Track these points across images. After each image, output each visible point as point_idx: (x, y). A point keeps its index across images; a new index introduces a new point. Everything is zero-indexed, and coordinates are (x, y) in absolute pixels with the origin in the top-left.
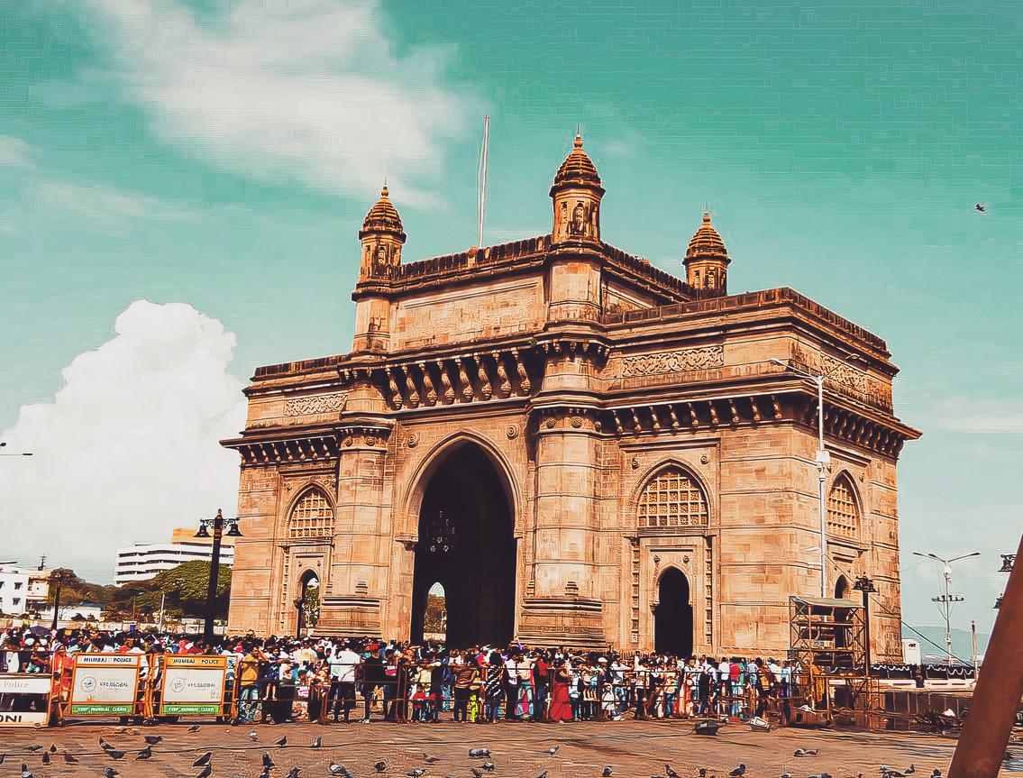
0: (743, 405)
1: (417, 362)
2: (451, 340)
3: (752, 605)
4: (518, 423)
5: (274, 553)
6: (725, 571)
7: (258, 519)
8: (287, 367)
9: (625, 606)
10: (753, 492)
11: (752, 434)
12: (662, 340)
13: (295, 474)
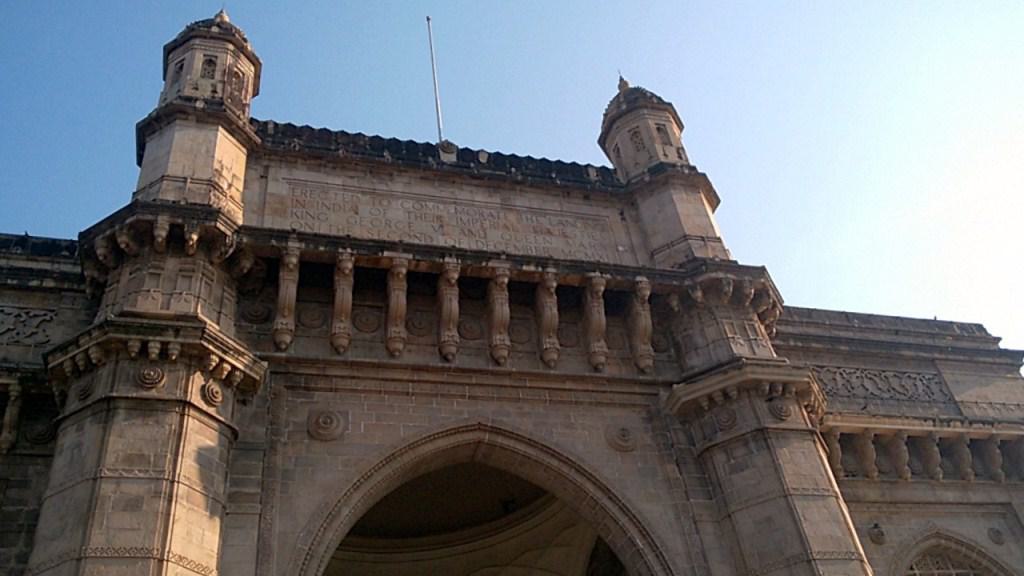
12: (843, 348)
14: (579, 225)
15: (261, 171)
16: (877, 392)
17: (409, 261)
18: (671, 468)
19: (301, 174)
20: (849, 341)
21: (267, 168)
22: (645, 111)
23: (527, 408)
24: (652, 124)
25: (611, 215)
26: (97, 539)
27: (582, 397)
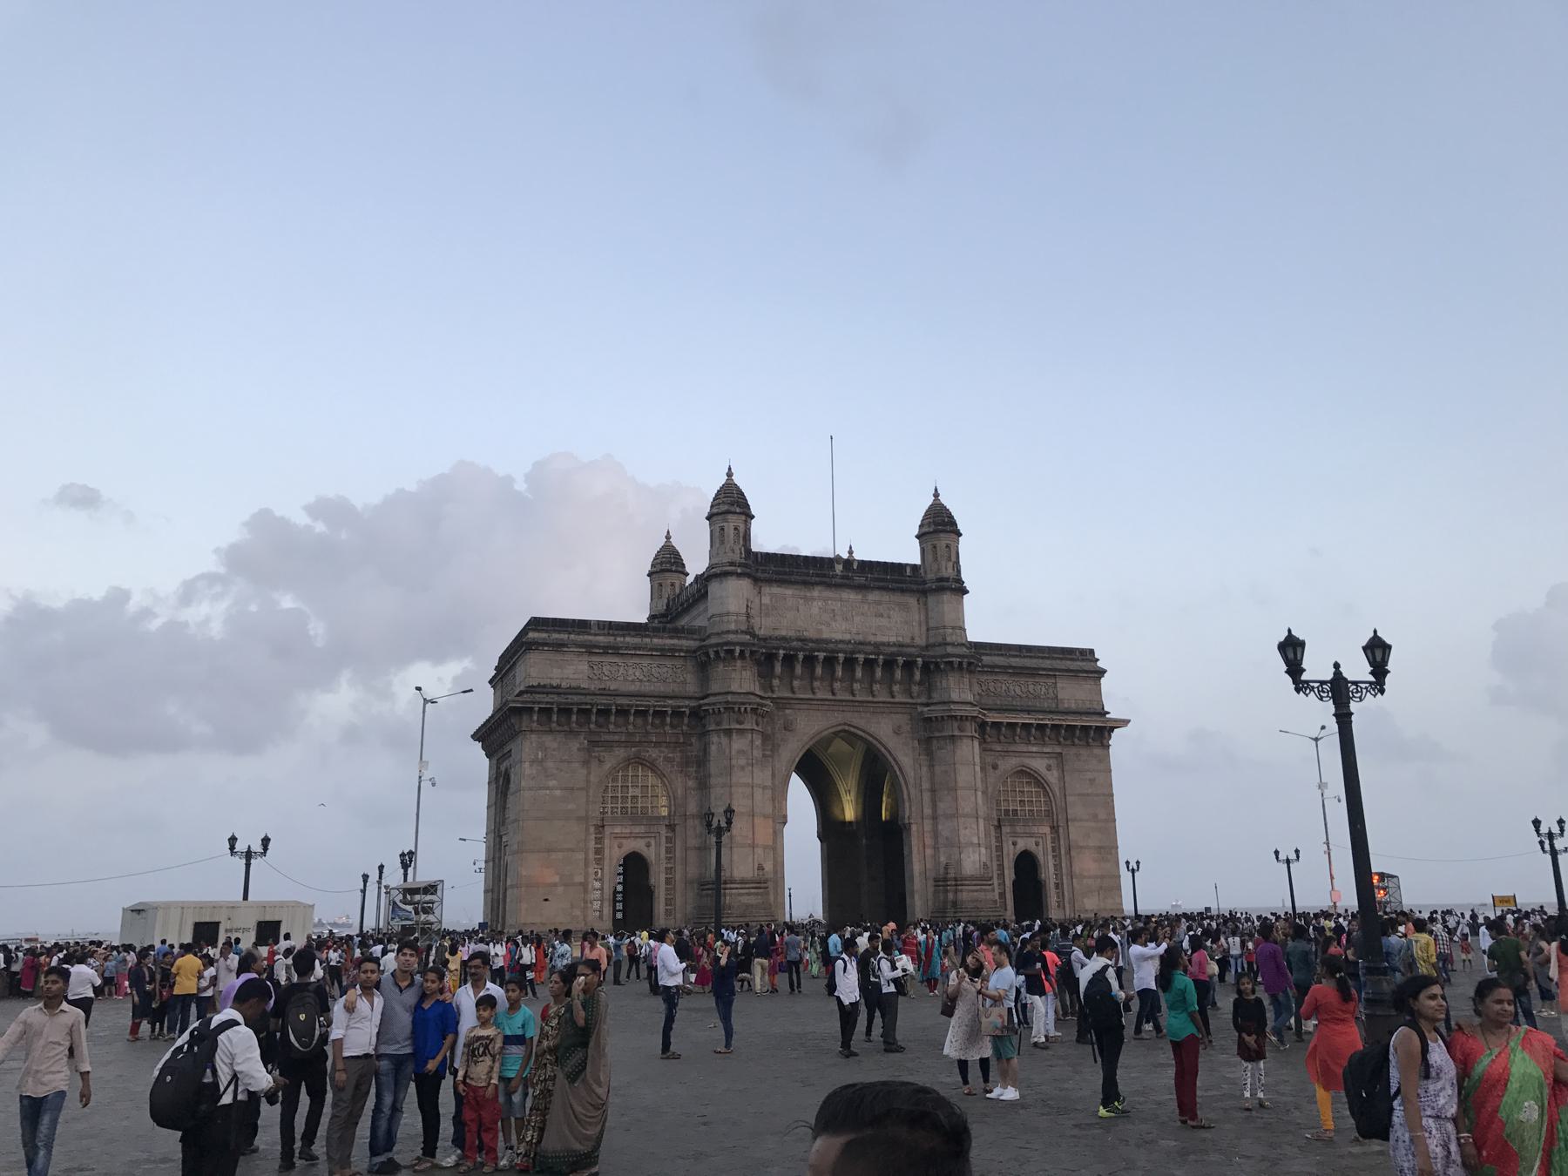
0: (1085, 729)
1: (816, 654)
2: (825, 635)
3: (1096, 877)
4: (902, 720)
5: (587, 830)
6: (1073, 853)
7: (558, 793)
8: (582, 626)
9: (996, 881)
10: (1088, 795)
11: (1084, 752)
12: (1010, 671)
13: (609, 745)
14: (897, 609)
15: (758, 589)
16: (1020, 693)
17: (825, 657)
18: (916, 742)
19: (776, 590)
20: (1014, 668)
21: (761, 587)
22: (942, 535)
23: (863, 714)
24: (943, 543)
25: (912, 601)
26: (734, 780)
27: (887, 710)
